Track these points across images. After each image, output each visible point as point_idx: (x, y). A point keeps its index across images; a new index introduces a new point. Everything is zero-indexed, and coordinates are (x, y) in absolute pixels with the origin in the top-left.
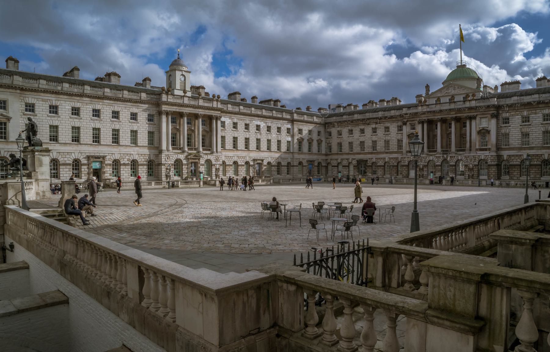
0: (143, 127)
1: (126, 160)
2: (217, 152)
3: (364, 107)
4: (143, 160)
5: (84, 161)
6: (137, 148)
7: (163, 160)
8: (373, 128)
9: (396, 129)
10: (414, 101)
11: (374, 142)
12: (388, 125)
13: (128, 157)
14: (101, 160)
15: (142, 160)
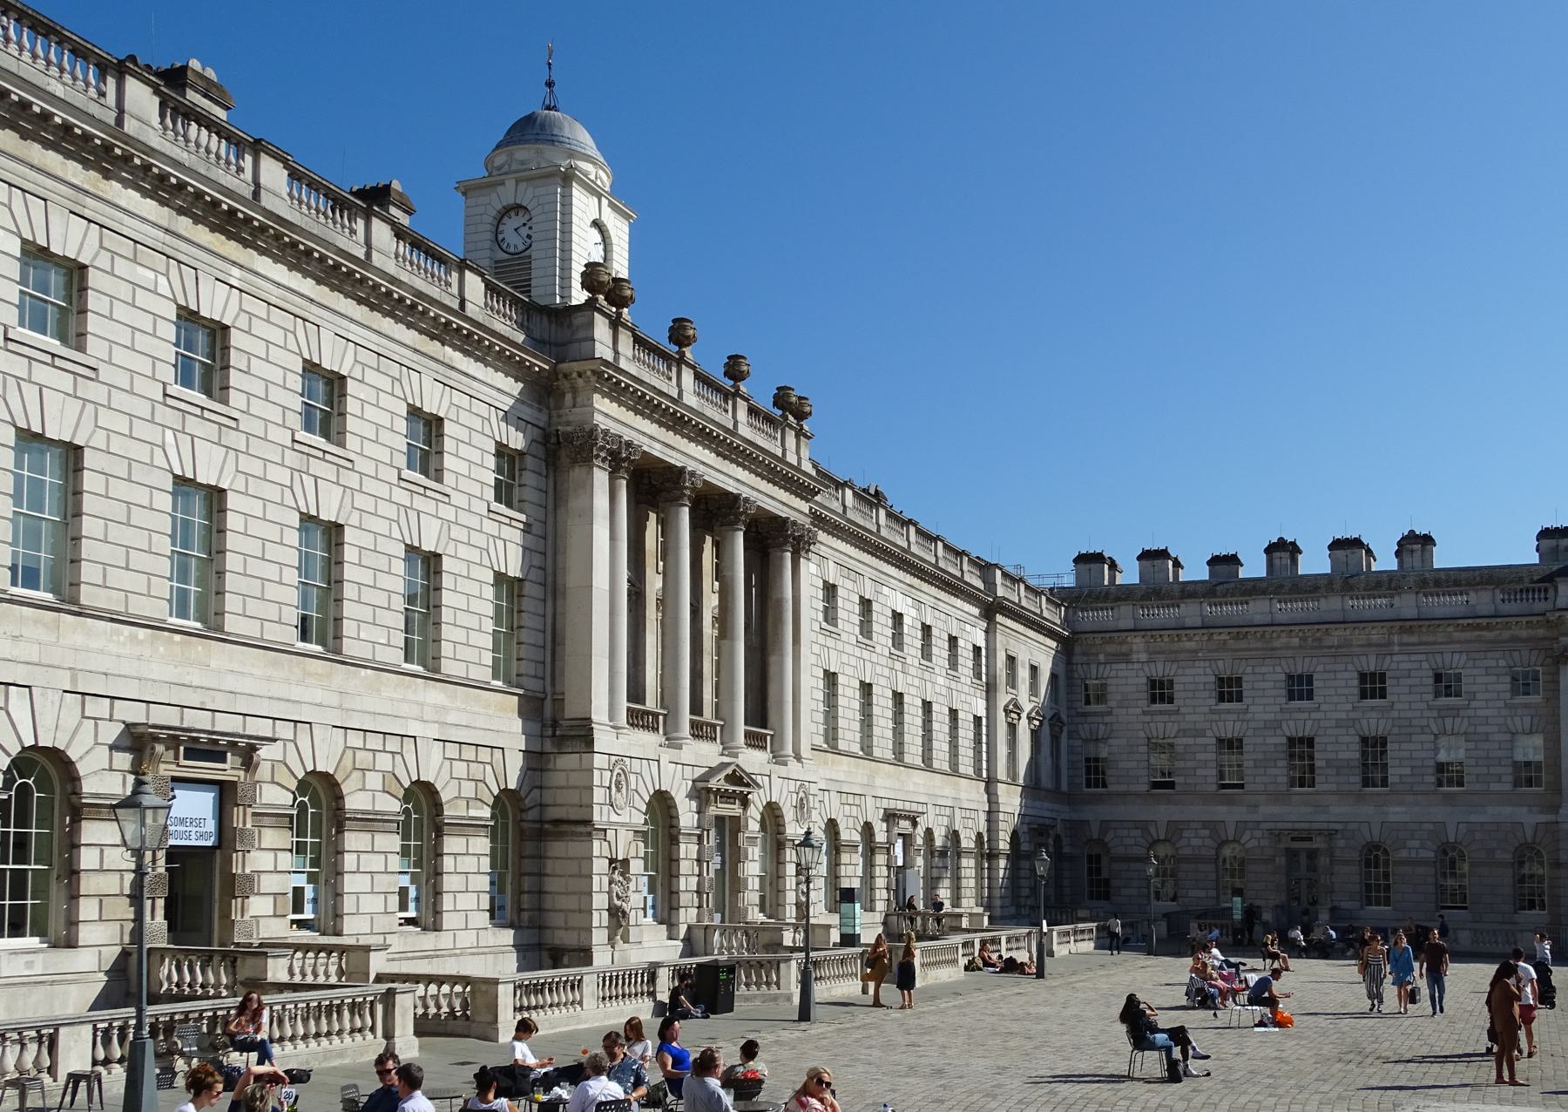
0: (483, 544)
1: (374, 781)
2: (798, 758)
3: (1223, 569)
4: (468, 789)
5: (103, 777)
6: (435, 694)
7: (599, 795)
8: (1363, 677)
9: (1505, 684)
10: (1526, 554)
11: (1374, 747)
12: (1454, 661)
13: (384, 762)
14: (229, 769)
15: (467, 796)
